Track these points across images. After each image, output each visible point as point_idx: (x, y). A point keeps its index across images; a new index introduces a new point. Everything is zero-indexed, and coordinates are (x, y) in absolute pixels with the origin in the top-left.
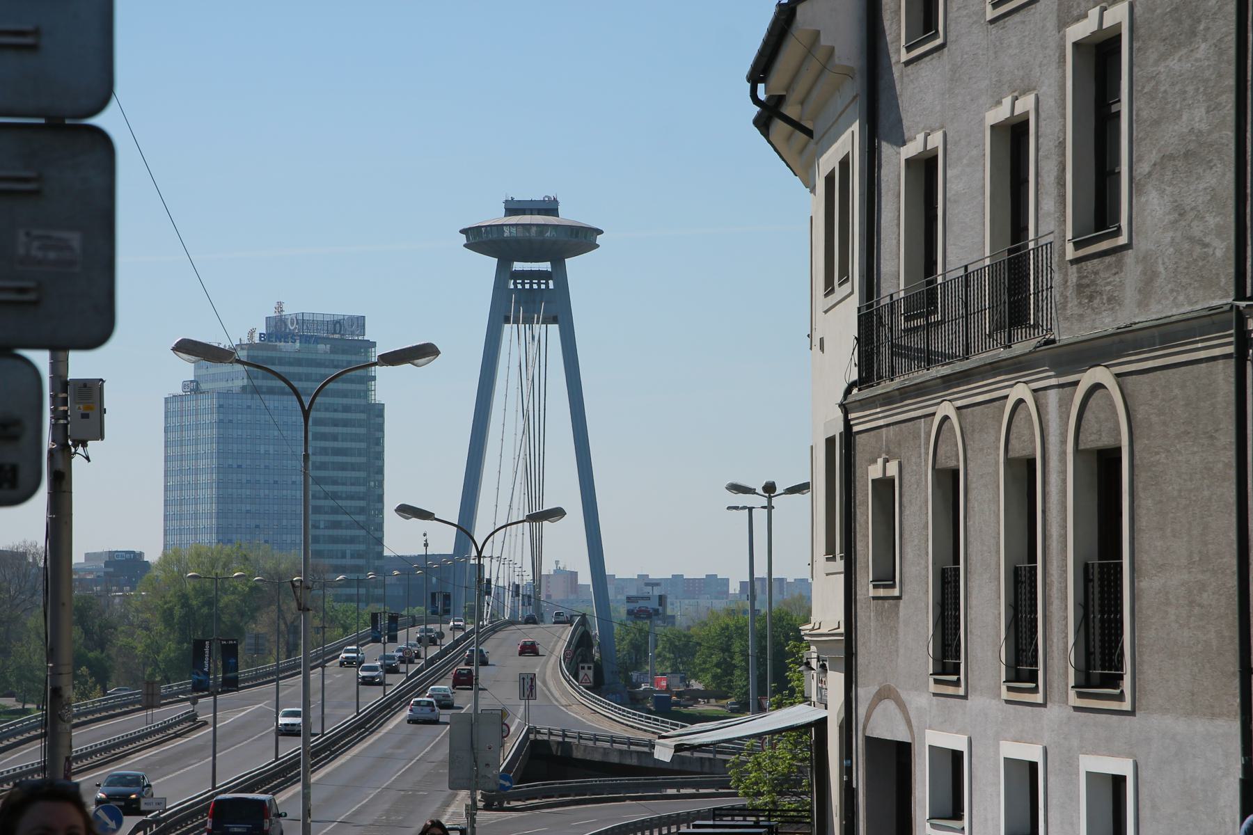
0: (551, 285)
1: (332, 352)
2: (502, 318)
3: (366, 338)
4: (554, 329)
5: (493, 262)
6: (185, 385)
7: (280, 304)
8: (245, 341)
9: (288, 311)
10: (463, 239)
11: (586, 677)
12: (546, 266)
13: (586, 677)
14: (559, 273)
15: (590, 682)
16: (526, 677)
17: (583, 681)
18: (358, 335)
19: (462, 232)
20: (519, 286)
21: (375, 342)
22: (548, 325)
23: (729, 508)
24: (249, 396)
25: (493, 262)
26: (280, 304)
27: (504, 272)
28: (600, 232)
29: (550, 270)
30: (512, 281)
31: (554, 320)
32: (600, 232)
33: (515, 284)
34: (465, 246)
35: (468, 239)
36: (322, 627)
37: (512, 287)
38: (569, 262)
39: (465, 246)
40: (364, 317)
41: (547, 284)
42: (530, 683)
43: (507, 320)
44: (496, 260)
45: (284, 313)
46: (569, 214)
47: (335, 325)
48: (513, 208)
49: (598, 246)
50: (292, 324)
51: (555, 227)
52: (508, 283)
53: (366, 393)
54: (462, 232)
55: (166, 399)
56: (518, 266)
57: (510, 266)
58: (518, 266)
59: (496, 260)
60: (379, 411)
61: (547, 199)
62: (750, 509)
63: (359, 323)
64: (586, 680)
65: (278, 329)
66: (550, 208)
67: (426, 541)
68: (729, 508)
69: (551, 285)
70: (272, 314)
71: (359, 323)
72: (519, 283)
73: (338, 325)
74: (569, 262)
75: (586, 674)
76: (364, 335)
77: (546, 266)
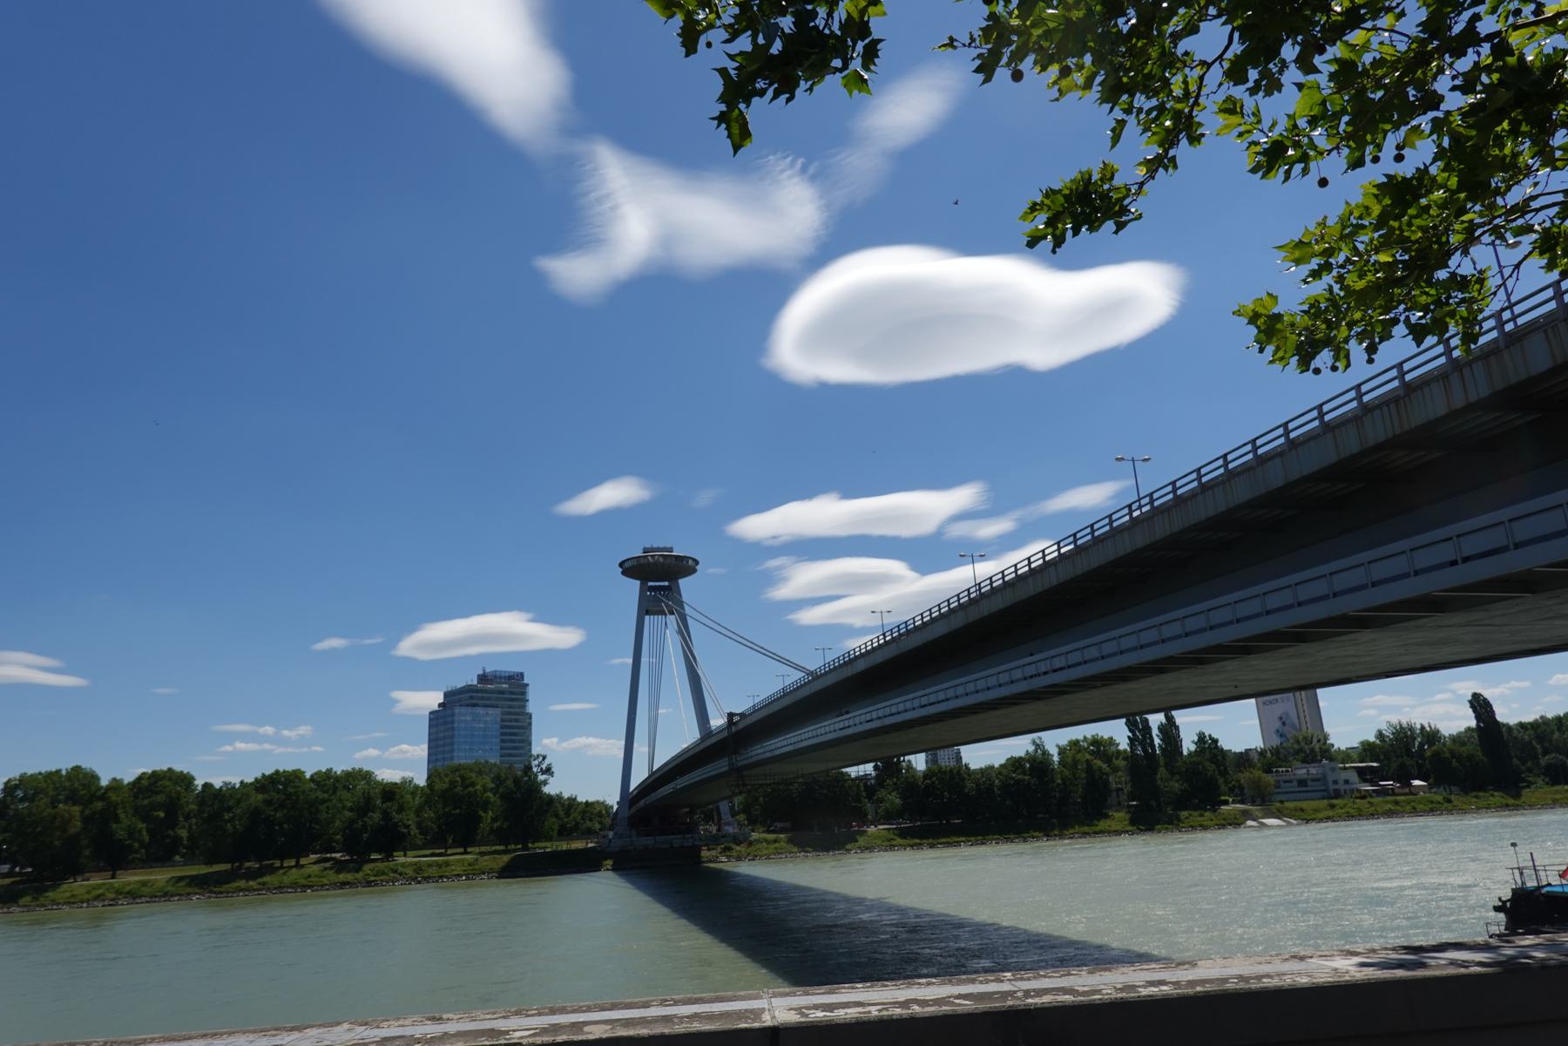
1: (509, 687)
2: (645, 612)
4: (672, 619)
6: (440, 705)
9: (487, 670)
12: (666, 583)
19: (621, 565)
25: (638, 583)
44: (639, 582)
48: (646, 550)
53: (524, 707)
56: (650, 584)
58: (650, 584)
59: (639, 582)
60: (530, 716)
63: (522, 675)
65: (483, 678)
66: (671, 550)
70: (481, 672)
71: (522, 675)
77: (666, 583)
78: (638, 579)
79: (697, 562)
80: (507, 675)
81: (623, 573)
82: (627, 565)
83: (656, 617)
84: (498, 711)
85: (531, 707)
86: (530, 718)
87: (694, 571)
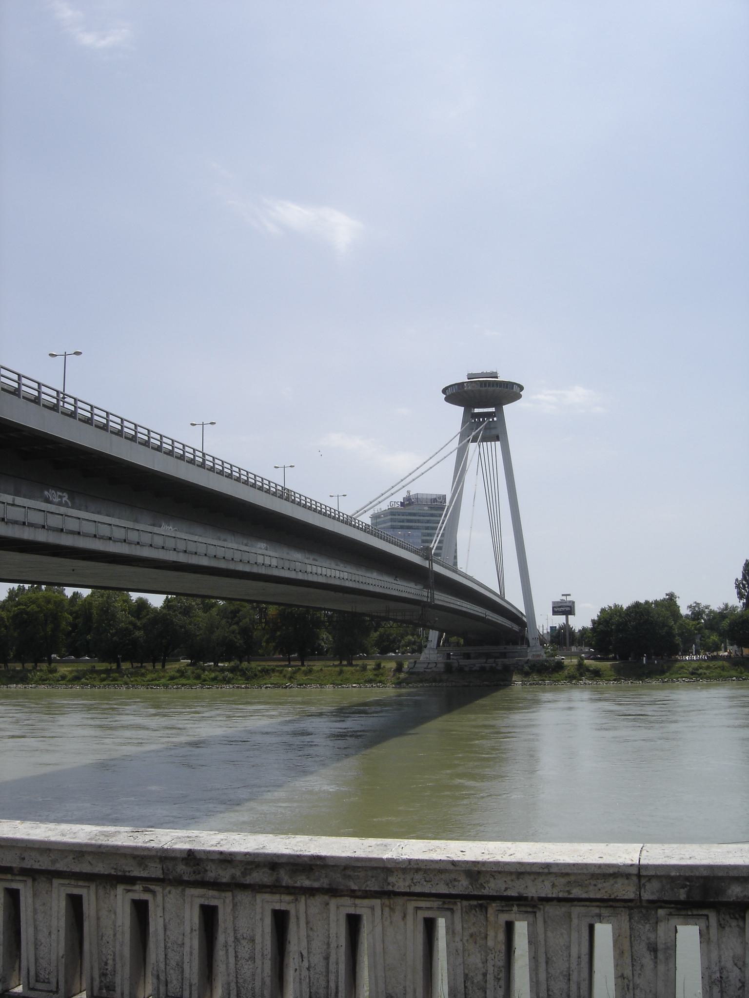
4: (498, 443)
5: (460, 410)
8: (390, 507)
12: (493, 410)
14: (500, 413)
27: (469, 416)
29: (494, 411)
31: (497, 438)
38: (506, 408)
44: (463, 408)
56: (476, 410)
58: (476, 410)
59: (463, 408)
69: (495, 419)
74: (506, 408)
77: (493, 410)
79: (521, 388)
80: (429, 497)
81: (447, 399)
82: (449, 392)
83: (489, 443)
84: (417, 533)
87: (519, 397)
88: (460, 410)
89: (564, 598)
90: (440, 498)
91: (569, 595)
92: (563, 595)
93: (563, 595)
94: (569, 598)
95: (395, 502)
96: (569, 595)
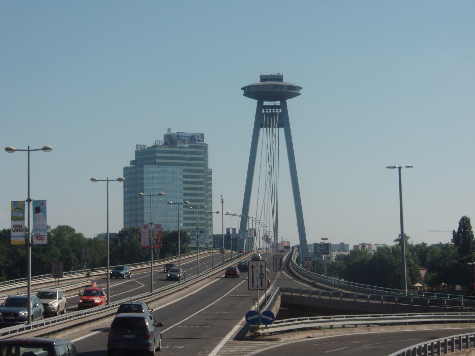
0: (280, 111)
3: (204, 142)
4: (282, 130)
6: (132, 163)
7: (169, 130)
8: (155, 145)
9: (172, 132)
10: (243, 92)
11: (308, 265)
12: (278, 103)
13: (308, 265)
14: (284, 106)
15: (310, 267)
16: (277, 258)
17: (307, 267)
18: (201, 142)
19: (243, 89)
20: (267, 112)
21: (208, 144)
22: (279, 128)
23: (387, 167)
24: (157, 166)
26: (169, 130)
27: (260, 107)
28: (301, 88)
29: (280, 104)
30: (264, 110)
32: (301, 88)
33: (265, 111)
34: (244, 95)
35: (245, 92)
36: (150, 224)
37: (264, 112)
39: (244, 95)
40: (203, 134)
41: (279, 110)
42: (280, 262)
43: (262, 126)
44: (257, 101)
45: (171, 133)
46: (288, 80)
47: (192, 138)
48: (263, 78)
49: (299, 94)
50: (175, 137)
51: (281, 86)
52: (262, 111)
54: (243, 89)
55: (124, 168)
56: (266, 103)
57: (263, 103)
58: (266, 103)
59: (257, 101)
61: (278, 75)
62: (400, 168)
64: (308, 266)
67: (222, 199)
68: (387, 167)
71: (202, 135)
72: (267, 110)
73: (193, 138)
75: (308, 263)
76: (203, 141)
77: (278, 103)
78: (256, 100)
80: (189, 135)
81: (245, 95)
84: (180, 169)
85: (211, 164)
86: (211, 173)
88: (254, 103)
89: (323, 241)
90: (198, 137)
91: (327, 239)
92: (322, 239)
93: (322, 239)
94: (327, 242)
95: (160, 141)
96: (327, 239)
